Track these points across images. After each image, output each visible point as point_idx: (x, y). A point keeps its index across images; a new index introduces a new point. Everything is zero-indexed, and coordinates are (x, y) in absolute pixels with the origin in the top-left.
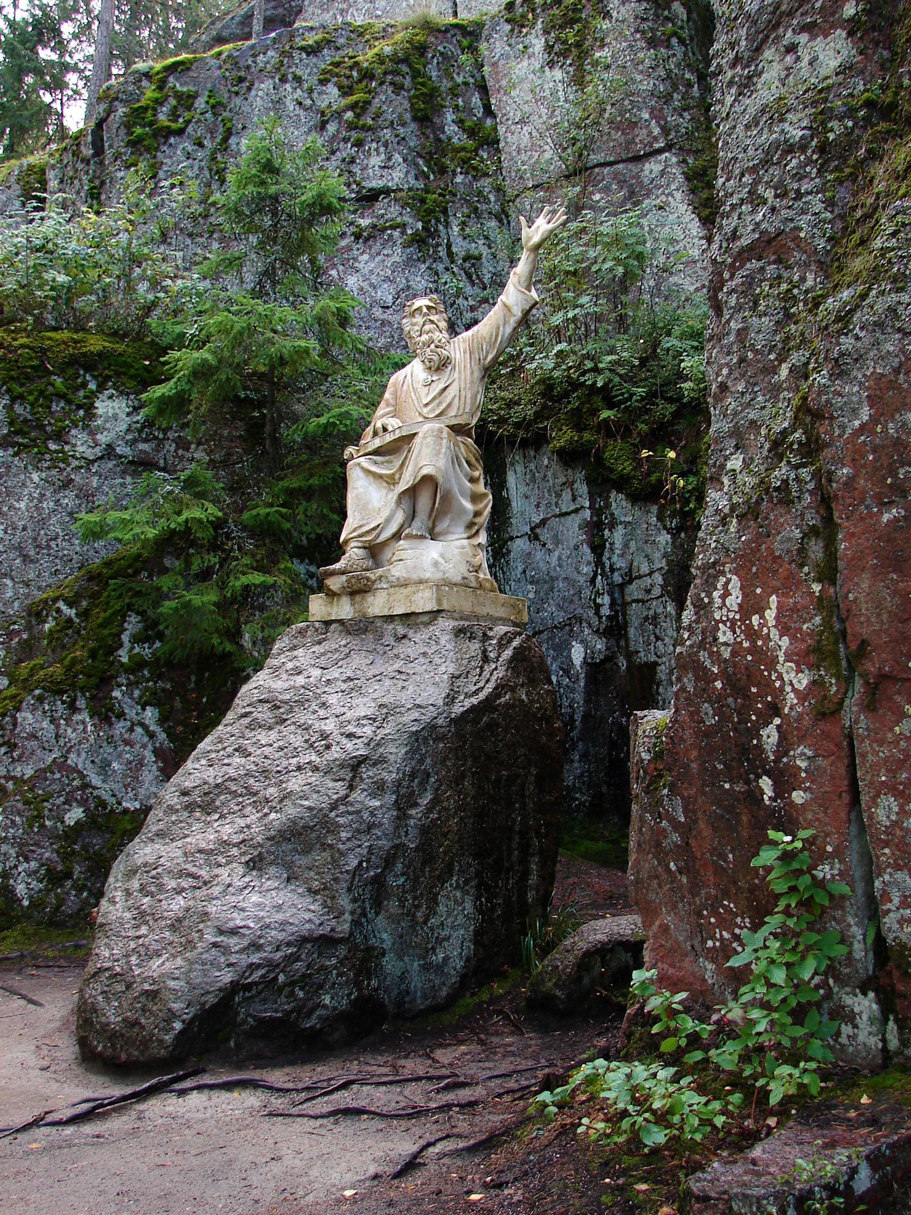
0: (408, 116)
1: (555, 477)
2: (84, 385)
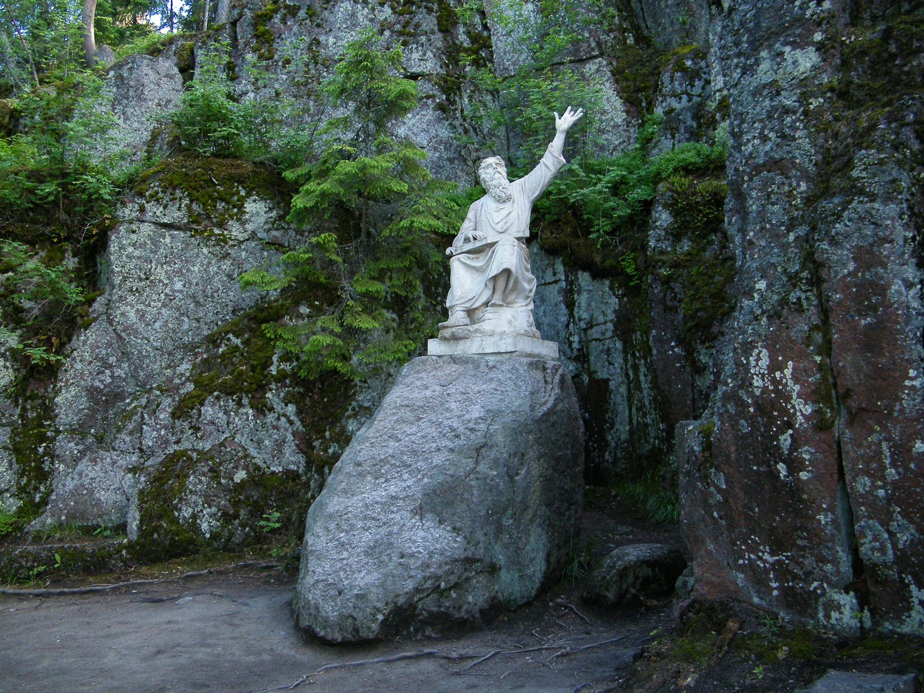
0: (436, 28)
1: (542, 260)
2: (238, 193)
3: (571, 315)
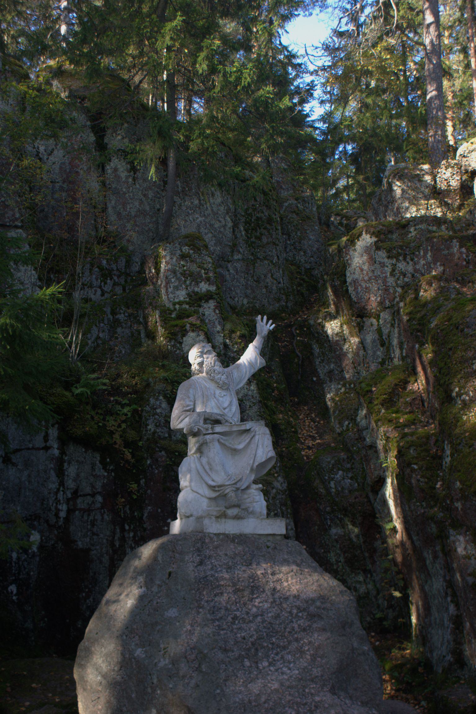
3: (62, 484)
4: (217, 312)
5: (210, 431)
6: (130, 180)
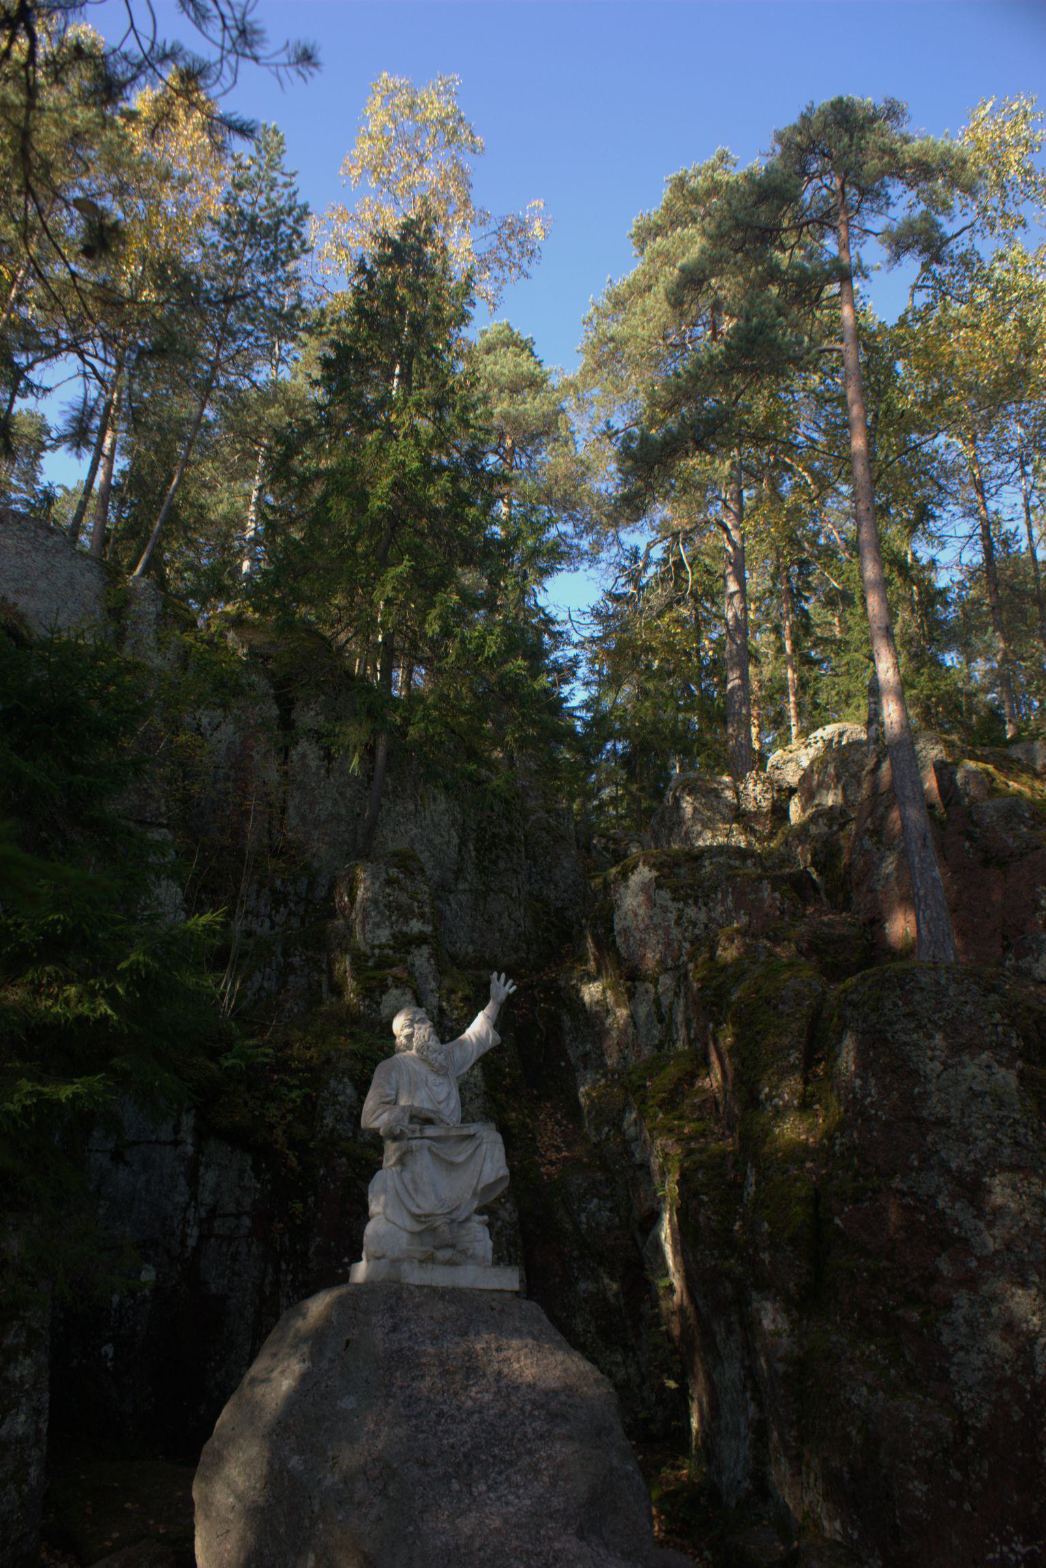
3: (194, 1196)
4: (432, 962)
5: (418, 1135)
6: (323, 772)
